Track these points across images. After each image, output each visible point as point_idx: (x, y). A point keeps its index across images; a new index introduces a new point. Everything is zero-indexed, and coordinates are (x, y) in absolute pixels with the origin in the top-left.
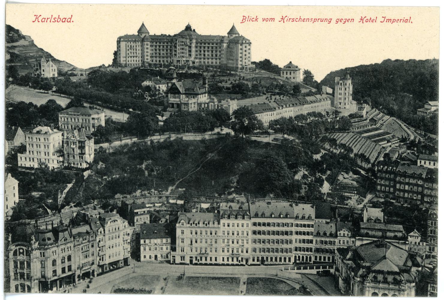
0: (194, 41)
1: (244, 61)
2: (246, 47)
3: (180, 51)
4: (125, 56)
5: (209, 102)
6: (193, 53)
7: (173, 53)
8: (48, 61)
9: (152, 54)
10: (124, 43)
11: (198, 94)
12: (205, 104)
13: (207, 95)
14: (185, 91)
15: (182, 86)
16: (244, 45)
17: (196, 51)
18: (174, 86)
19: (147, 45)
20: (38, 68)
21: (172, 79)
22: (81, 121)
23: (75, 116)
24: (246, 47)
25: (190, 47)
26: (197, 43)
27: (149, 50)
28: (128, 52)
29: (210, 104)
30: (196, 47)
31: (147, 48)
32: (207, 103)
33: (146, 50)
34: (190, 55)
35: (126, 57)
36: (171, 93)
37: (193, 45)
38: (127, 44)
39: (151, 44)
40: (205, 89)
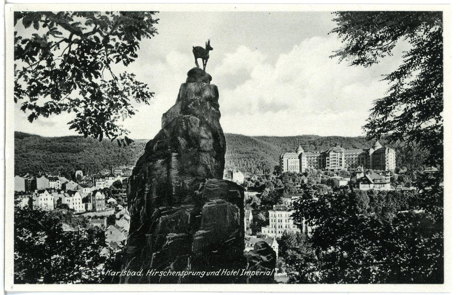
0: (343, 154)
3: (333, 162)
6: (343, 163)
7: (327, 165)
8: (237, 171)
17: (345, 162)
25: (341, 159)
30: (345, 159)
31: (304, 162)
33: (303, 164)
34: (341, 165)
37: (343, 157)
38: (289, 160)
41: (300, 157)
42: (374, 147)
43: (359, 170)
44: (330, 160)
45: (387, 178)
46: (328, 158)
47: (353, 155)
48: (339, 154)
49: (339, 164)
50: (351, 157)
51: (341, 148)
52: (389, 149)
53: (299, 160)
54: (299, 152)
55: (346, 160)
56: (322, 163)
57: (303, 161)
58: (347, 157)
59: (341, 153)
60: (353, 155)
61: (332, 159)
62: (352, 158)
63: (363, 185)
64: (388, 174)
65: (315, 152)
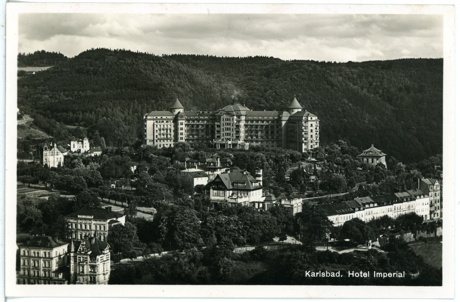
0: (243, 118)
1: (310, 144)
2: (312, 126)
4: (152, 138)
5: (265, 201)
6: (242, 135)
8: (51, 148)
9: (188, 136)
10: (152, 122)
11: (250, 190)
12: (259, 203)
13: (261, 190)
14: (233, 184)
15: (229, 179)
16: (310, 123)
18: (217, 180)
19: (182, 124)
20: (40, 156)
21: (215, 169)
22: (93, 227)
23: (86, 222)
24: (312, 126)
25: (238, 126)
26: (246, 121)
27: (183, 131)
28: (156, 134)
29: (266, 203)
30: (246, 126)
31: (182, 129)
32: (262, 203)
33: (180, 131)
34: (238, 138)
35: (153, 141)
36: (214, 189)
37: (242, 124)
38: (155, 123)
39: (186, 123)
40: (260, 184)
41: (175, 121)
42: (289, 110)
43: (212, 164)
44: (222, 127)
45: (258, 178)
46: (219, 124)
47: (263, 121)
48: (235, 117)
49: (235, 135)
50: (255, 123)
51: (241, 108)
52: (309, 114)
53: (172, 124)
54: (177, 111)
55: (247, 129)
56: (210, 131)
57: (180, 126)
58: (249, 123)
59: (239, 116)
60: (263, 121)
61: (225, 126)
62: (257, 126)
63: (215, 192)
64: (259, 173)
65: (201, 112)
